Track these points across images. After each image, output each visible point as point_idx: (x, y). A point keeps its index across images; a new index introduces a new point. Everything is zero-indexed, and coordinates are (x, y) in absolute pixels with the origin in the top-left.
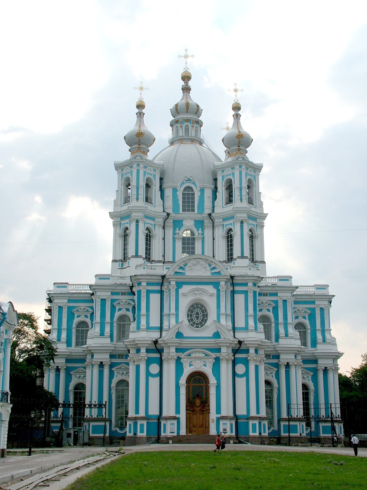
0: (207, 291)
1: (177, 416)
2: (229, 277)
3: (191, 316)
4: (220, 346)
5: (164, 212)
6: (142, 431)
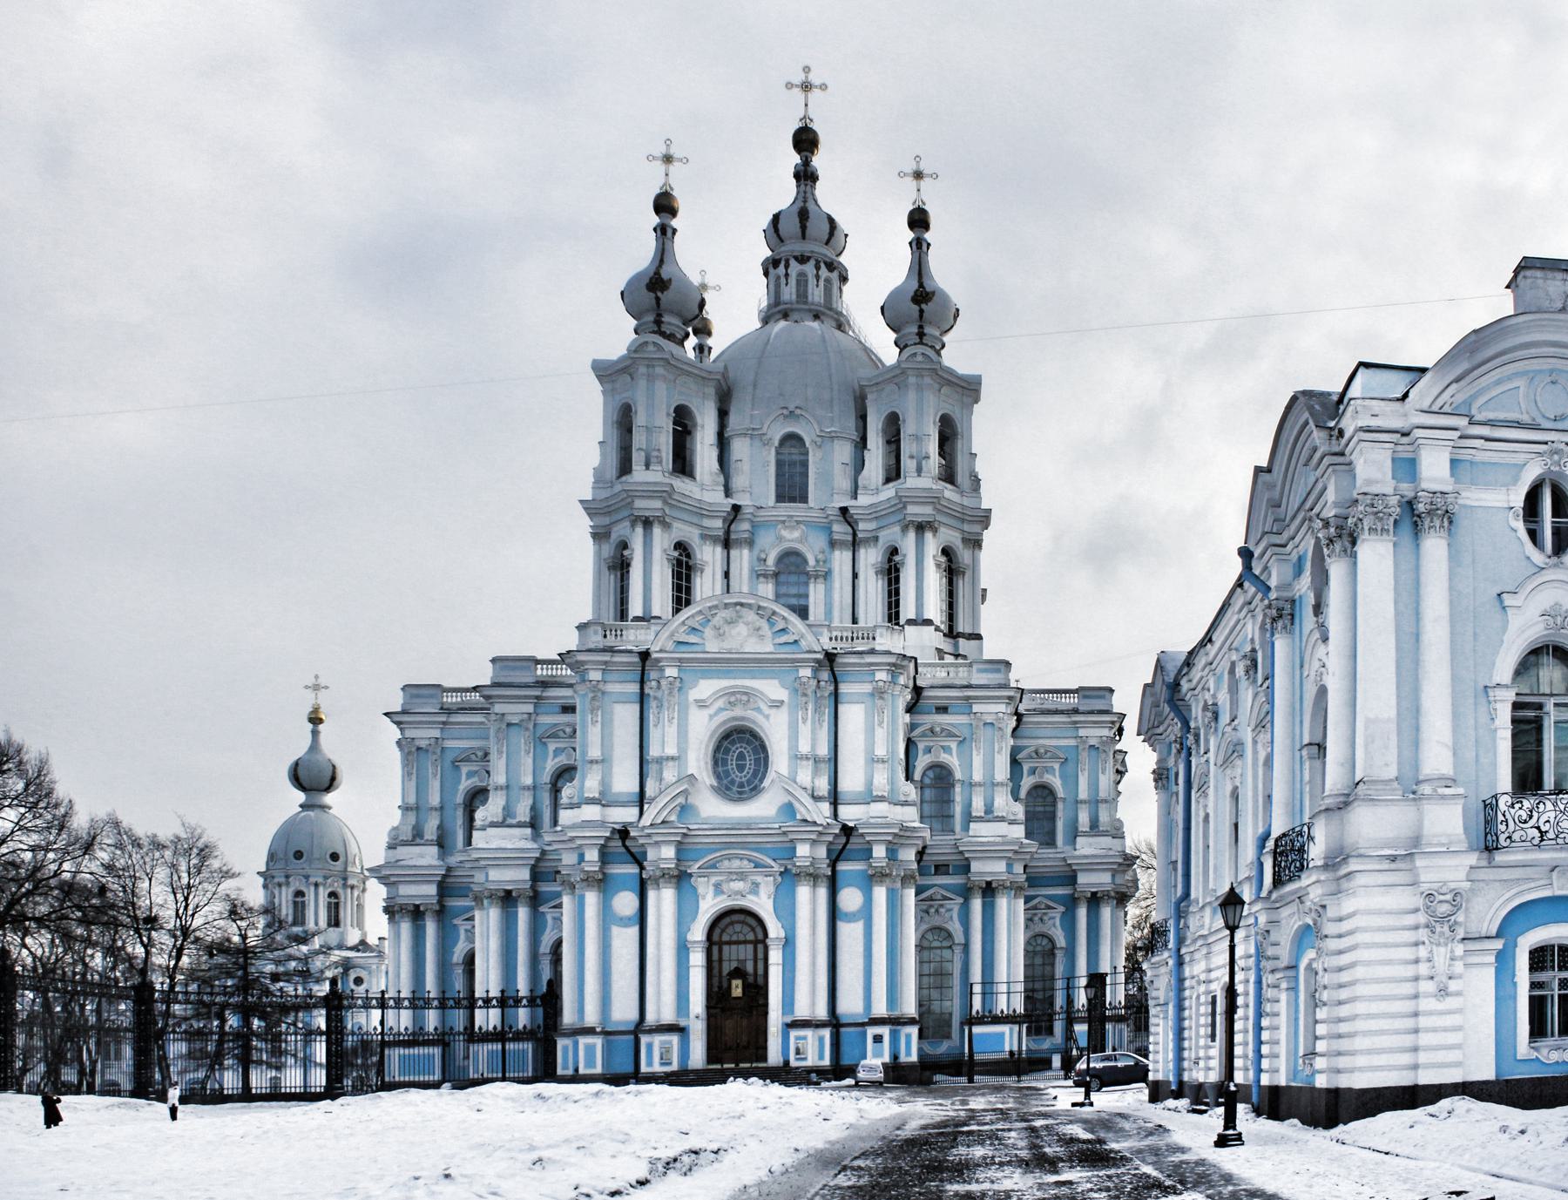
0: (762, 693)
2: (820, 656)
3: (725, 763)
4: (792, 841)
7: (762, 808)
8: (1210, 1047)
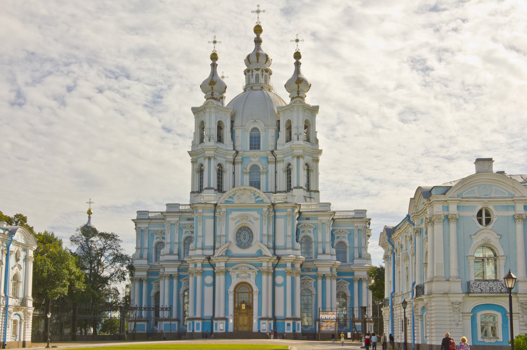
1: (227, 317)
3: (240, 237)
4: (261, 261)
5: (234, 150)
6: (198, 328)
7: (252, 250)
8: (402, 333)
